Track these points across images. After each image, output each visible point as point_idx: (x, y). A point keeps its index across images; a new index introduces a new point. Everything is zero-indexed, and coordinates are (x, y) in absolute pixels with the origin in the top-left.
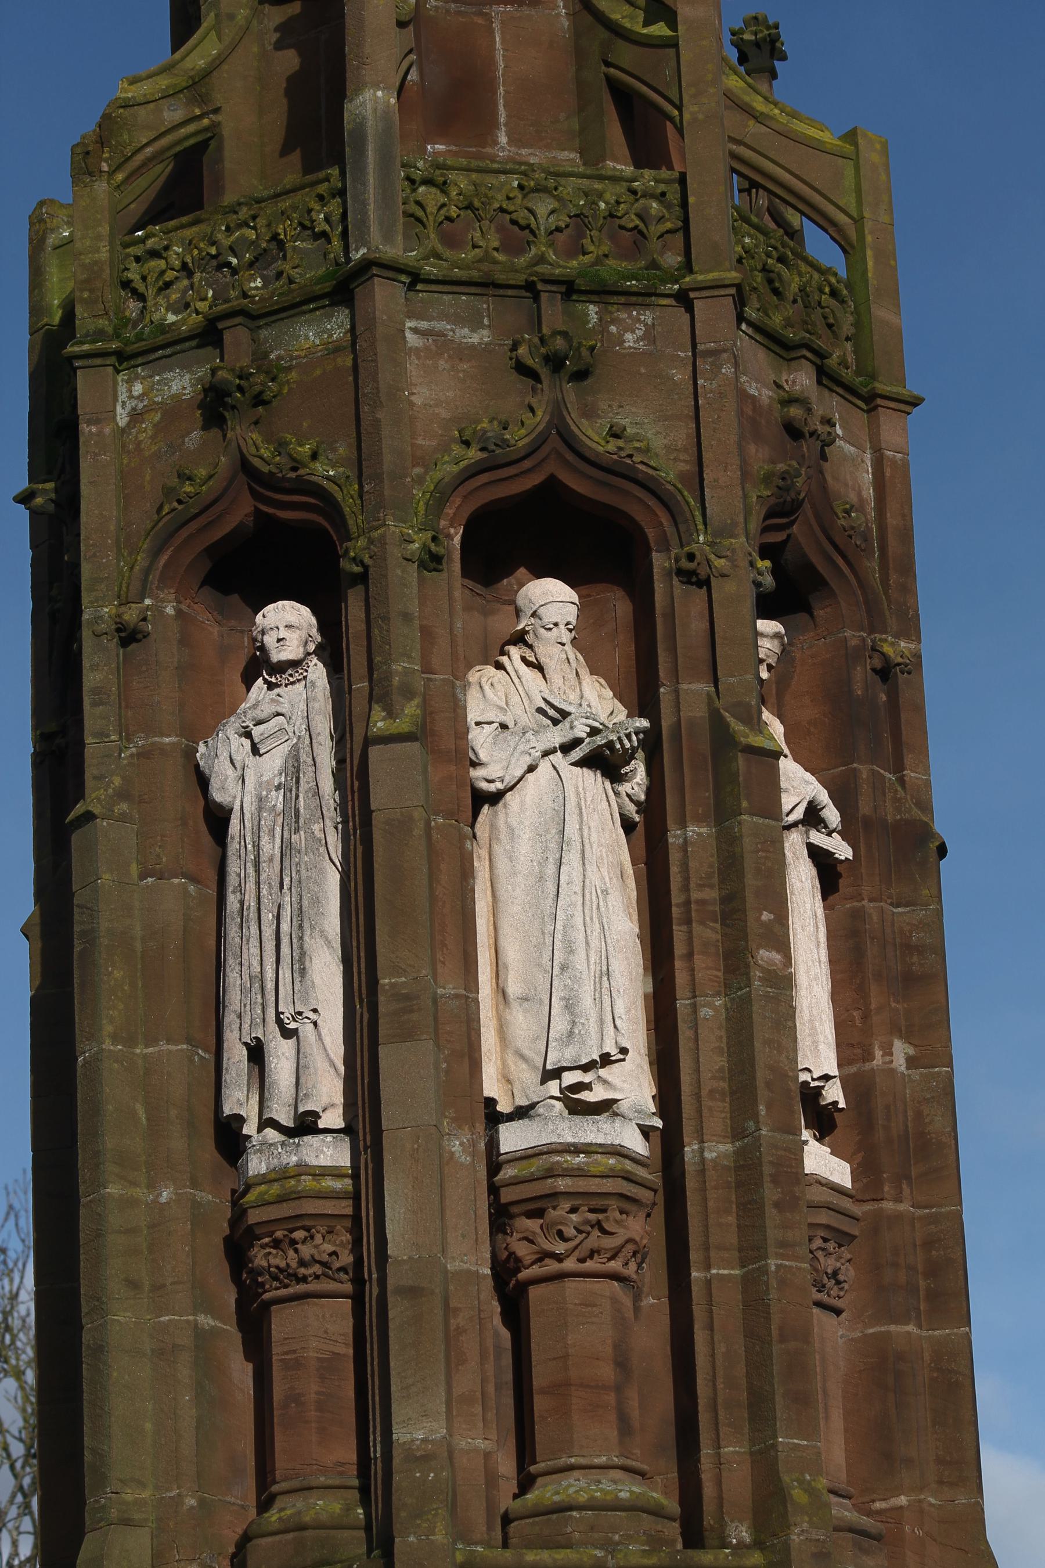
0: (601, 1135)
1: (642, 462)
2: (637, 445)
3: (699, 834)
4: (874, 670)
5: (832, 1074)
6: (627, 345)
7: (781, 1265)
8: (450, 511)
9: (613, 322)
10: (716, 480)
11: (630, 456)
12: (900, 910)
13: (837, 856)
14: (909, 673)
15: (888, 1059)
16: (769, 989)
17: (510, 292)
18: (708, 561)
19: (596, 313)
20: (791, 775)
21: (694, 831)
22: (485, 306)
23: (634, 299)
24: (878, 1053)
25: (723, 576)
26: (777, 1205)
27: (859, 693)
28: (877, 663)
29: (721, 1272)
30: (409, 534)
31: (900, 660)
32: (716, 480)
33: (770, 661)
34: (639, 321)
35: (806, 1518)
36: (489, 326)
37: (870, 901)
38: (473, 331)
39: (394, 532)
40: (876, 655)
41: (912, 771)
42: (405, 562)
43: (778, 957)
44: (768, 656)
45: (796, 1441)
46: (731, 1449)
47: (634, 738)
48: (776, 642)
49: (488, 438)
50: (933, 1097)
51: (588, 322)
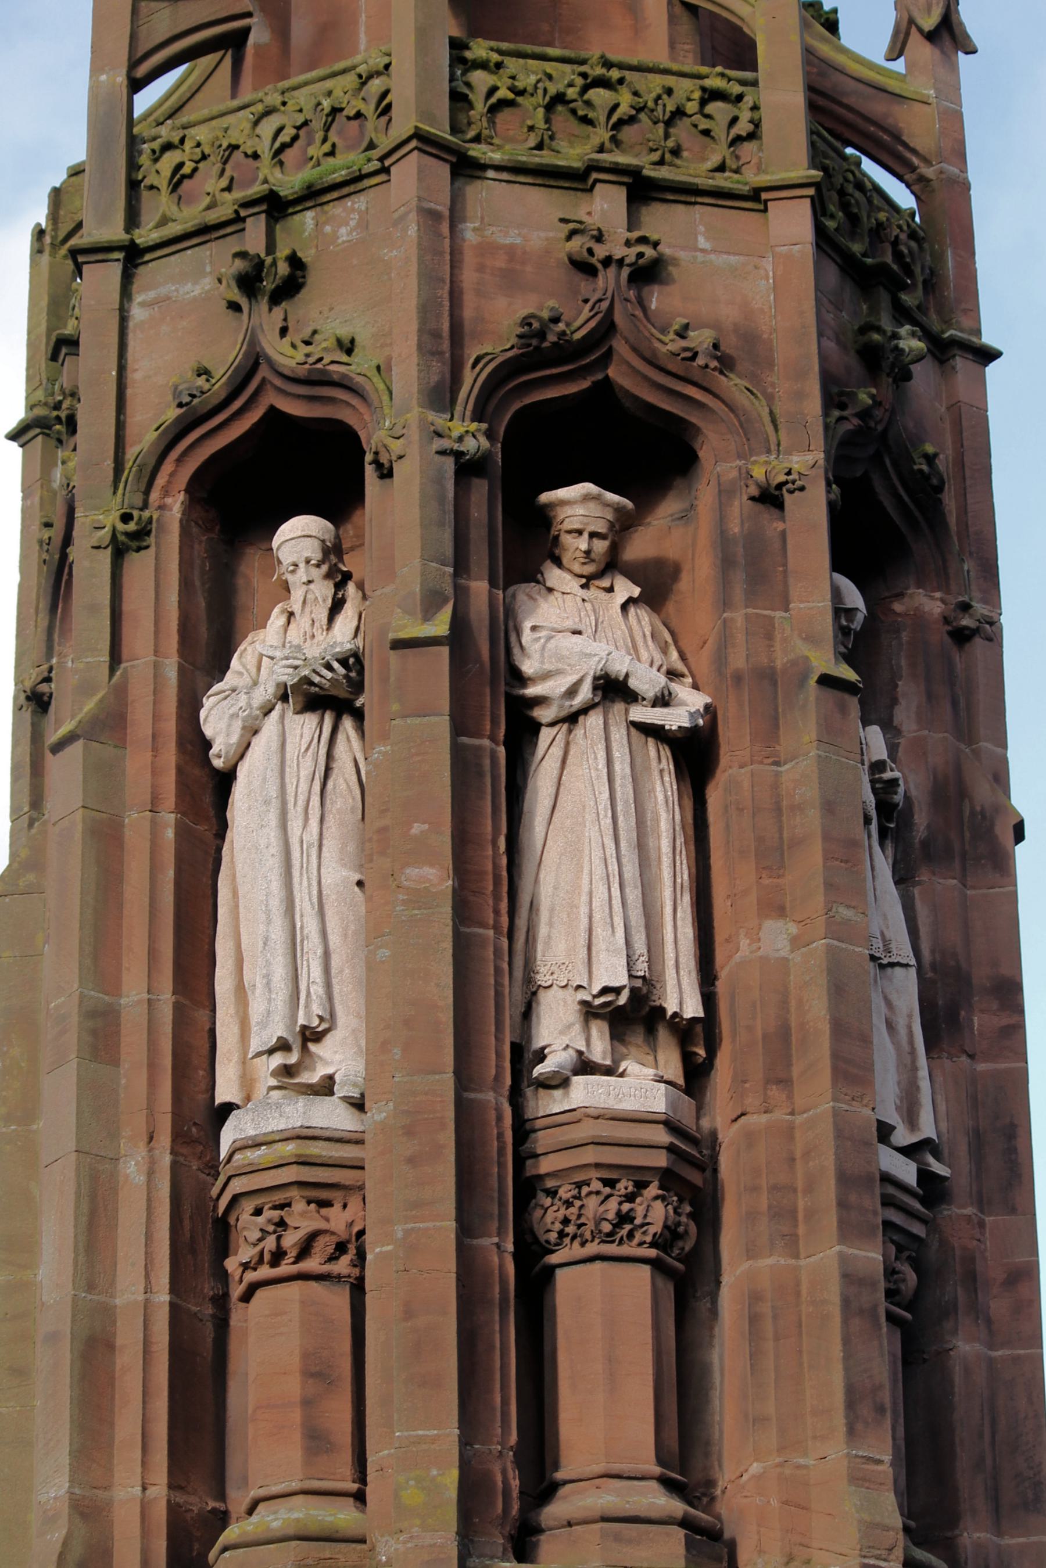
0: (283, 1120)
1: (333, 362)
2: (324, 345)
3: (385, 754)
4: (752, 499)
5: (617, 985)
6: (340, 241)
7: (412, 1229)
8: (161, 480)
9: (325, 223)
10: (400, 355)
11: (321, 359)
12: (787, 767)
13: (667, 727)
14: (802, 489)
15: (755, 946)
16: (416, 912)
17: (229, 230)
18: (385, 446)
19: (313, 219)
20: (565, 653)
21: (379, 753)
22: (208, 253)
23: (345, 190)
24: (744, 943)
25: (401, 457)
26: (411, 1161)
27: (736, 530)
28: (754, 491)
29: (385, 1249)
30: (99, 521)
31: (782, 478)
32: (400, 355)
33: (592, 528)
34: (353, 210)
35: (418, 1522)
36: (211, 273)
37: (741, 767)
38: (195, 283)
39: (83, 523)
40: (750, 482)
41: (802, 602)
42: (95, 551)
43: (432, 871)
44: (588, 524)
45: (420, 1432)
46: (386, 1452)
47: (336, 665)
48: (592, 505)
49: (181, 392)
50: (811, 978)
51: (304, 231)
